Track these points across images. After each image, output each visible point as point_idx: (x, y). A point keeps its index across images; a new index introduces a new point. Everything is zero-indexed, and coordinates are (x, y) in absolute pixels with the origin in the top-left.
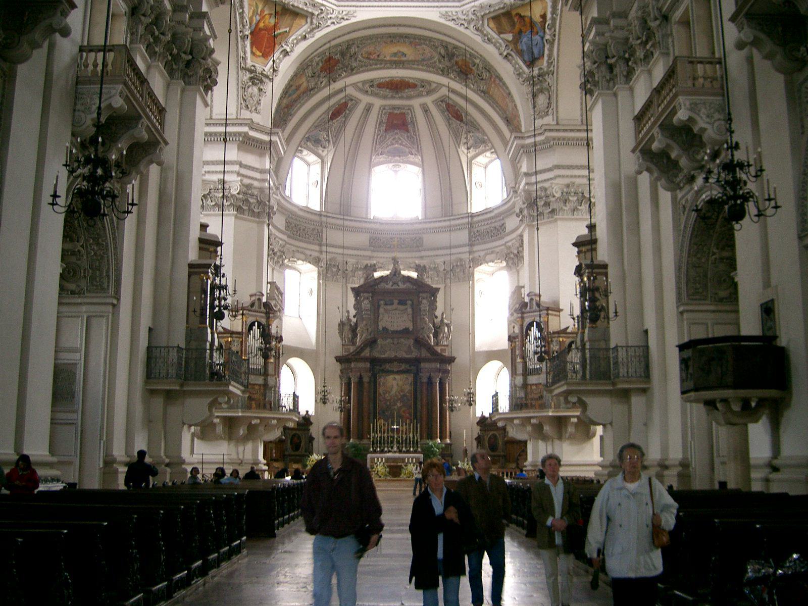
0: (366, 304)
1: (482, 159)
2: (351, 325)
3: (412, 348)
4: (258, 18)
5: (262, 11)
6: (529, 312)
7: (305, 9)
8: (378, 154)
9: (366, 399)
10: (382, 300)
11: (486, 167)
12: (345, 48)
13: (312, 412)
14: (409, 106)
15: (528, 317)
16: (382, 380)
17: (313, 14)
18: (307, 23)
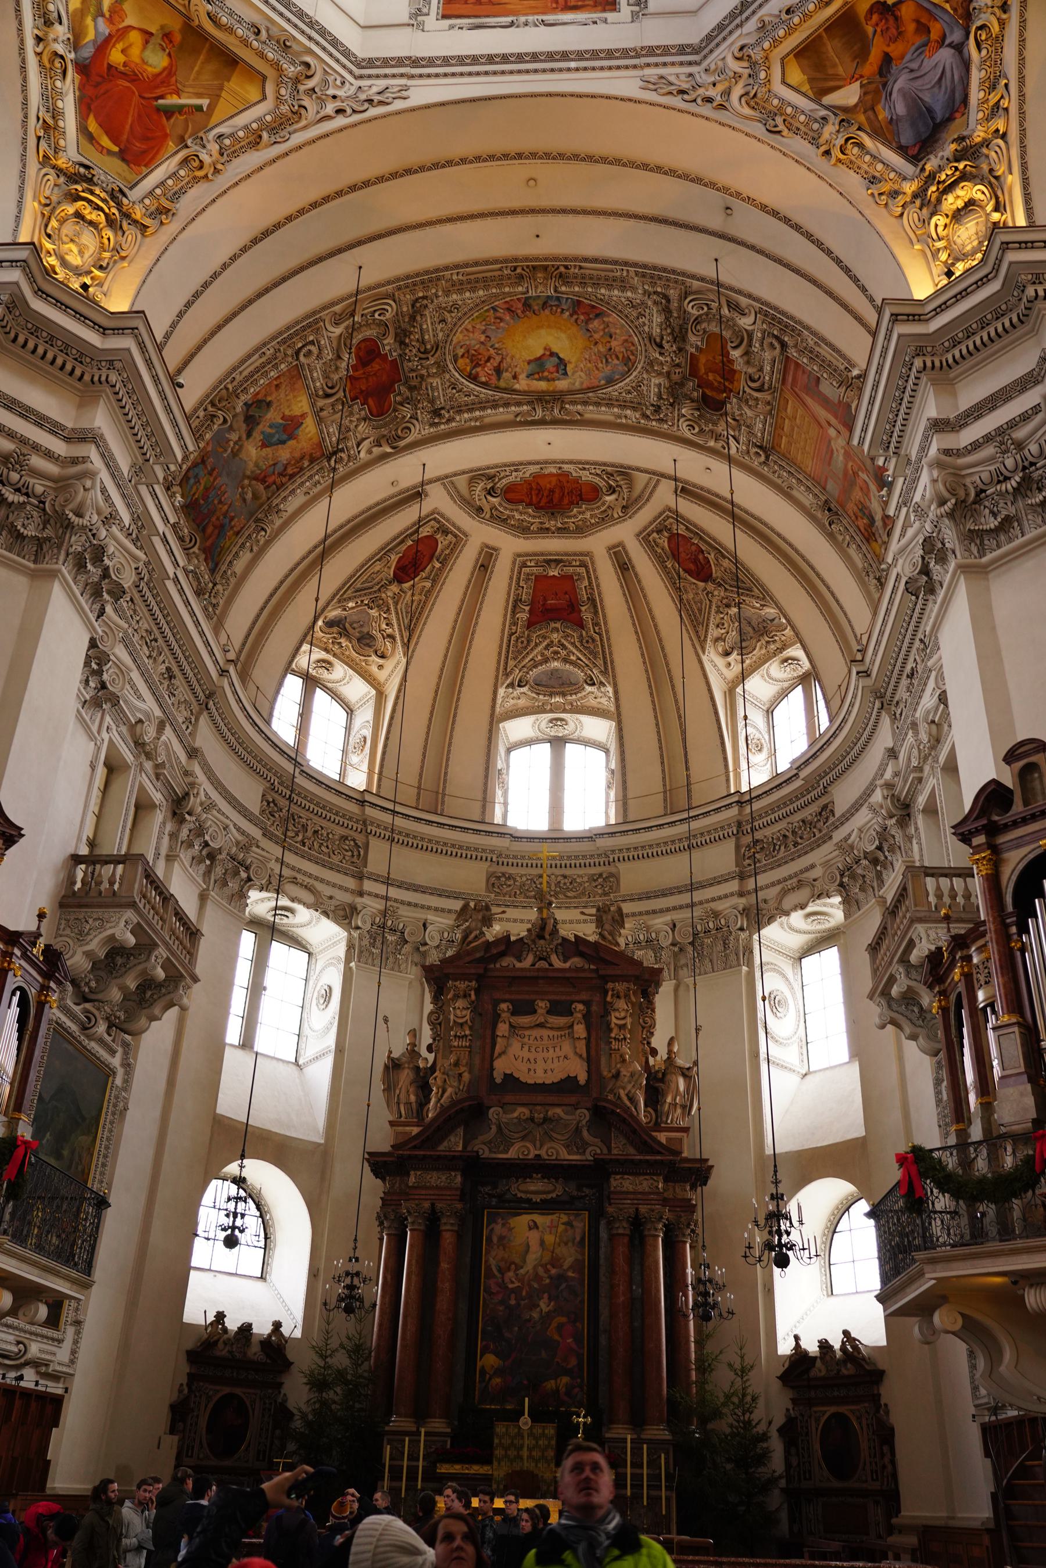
0: (459, 1010)
1: (759, 687)
2: (418, 1068)
3: (585, 1133)
4: (104, 28)
6: (1025, 821)
7: (255, 44)
8: (511, 685)
9: (445, 1286)
10: (505, 1001)
11: (769, 712)
12: (405, 309)
13: (293, 1327)
14: (582, 554)
15: (1019, 842)
16: (498, 1229)
18: (264, 98)
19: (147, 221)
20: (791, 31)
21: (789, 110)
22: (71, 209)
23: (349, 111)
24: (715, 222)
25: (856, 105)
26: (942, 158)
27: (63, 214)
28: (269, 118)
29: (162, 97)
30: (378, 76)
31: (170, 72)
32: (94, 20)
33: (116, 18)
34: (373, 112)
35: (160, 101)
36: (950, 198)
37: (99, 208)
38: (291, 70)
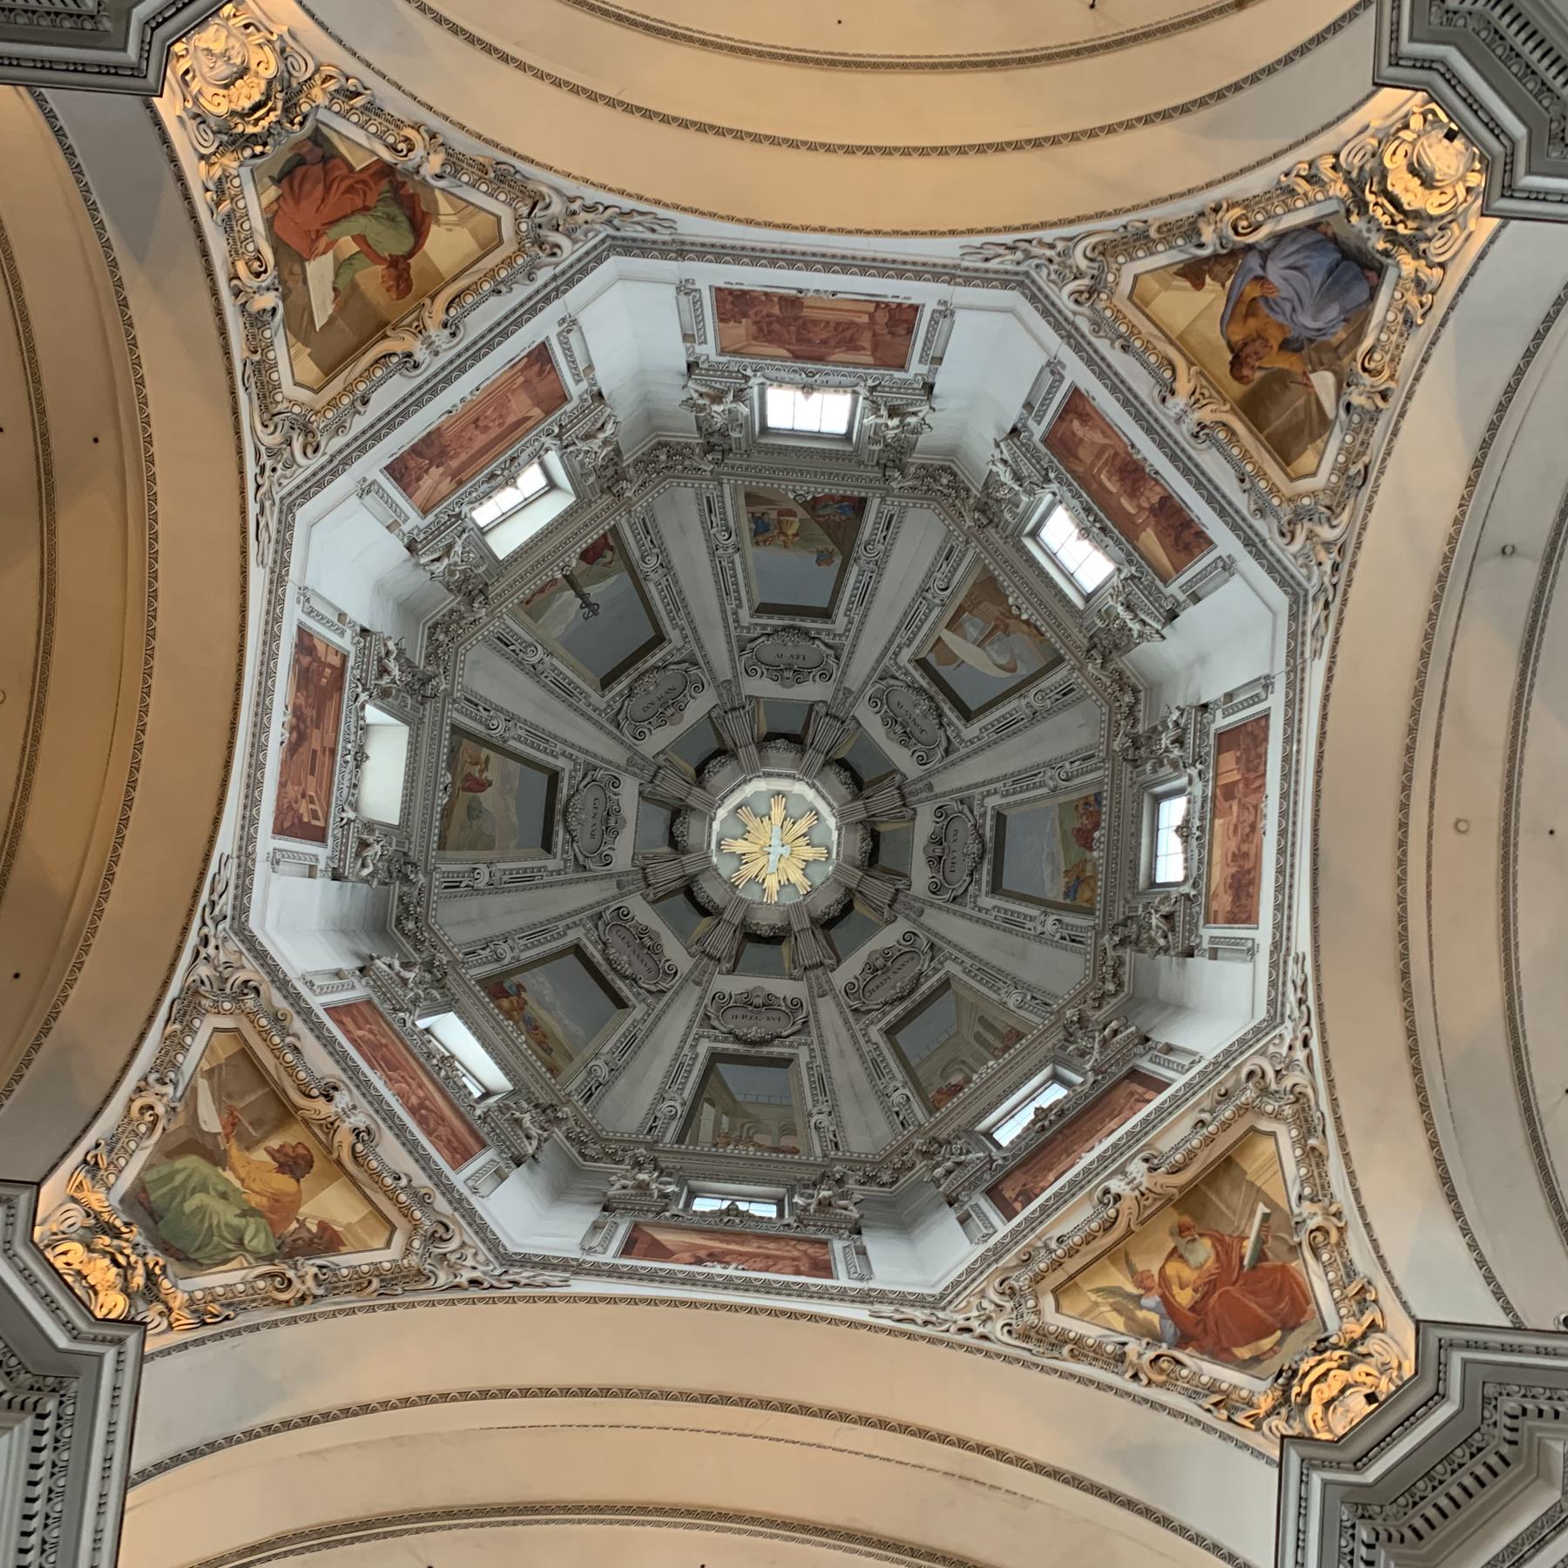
4: (1152, 1300)
5: (1140, 1279)
7: (1212, 1128)
17: (1244, 1109)
19: (1366, 1320)
20: (1261, 473)
21: (1341, 459)
22: (1315, 1408)
23: (1306, 1031)
24: (1527, 571)
25: (1334, 372)
26: (1369, 230)
27: (1320, 1424)
28: (1294, 1133)
29: (1242, 1259)
30: (1284, 994)
31: (1219, 1241)
32: (1141, 1308)
33: (1148, 1283)
34: (1311, 1002)
35: (1246, 1262)
36: (1405, 199)
37: (1325, 1374)
38: (1250, 1094)
